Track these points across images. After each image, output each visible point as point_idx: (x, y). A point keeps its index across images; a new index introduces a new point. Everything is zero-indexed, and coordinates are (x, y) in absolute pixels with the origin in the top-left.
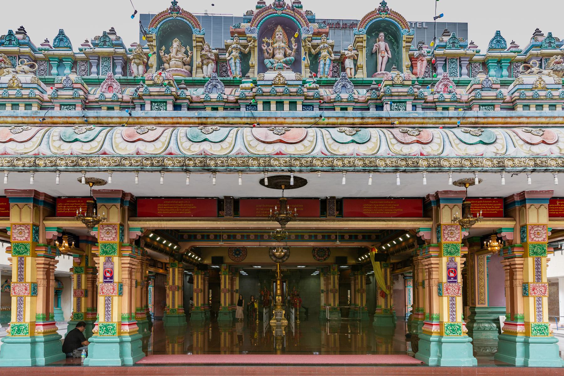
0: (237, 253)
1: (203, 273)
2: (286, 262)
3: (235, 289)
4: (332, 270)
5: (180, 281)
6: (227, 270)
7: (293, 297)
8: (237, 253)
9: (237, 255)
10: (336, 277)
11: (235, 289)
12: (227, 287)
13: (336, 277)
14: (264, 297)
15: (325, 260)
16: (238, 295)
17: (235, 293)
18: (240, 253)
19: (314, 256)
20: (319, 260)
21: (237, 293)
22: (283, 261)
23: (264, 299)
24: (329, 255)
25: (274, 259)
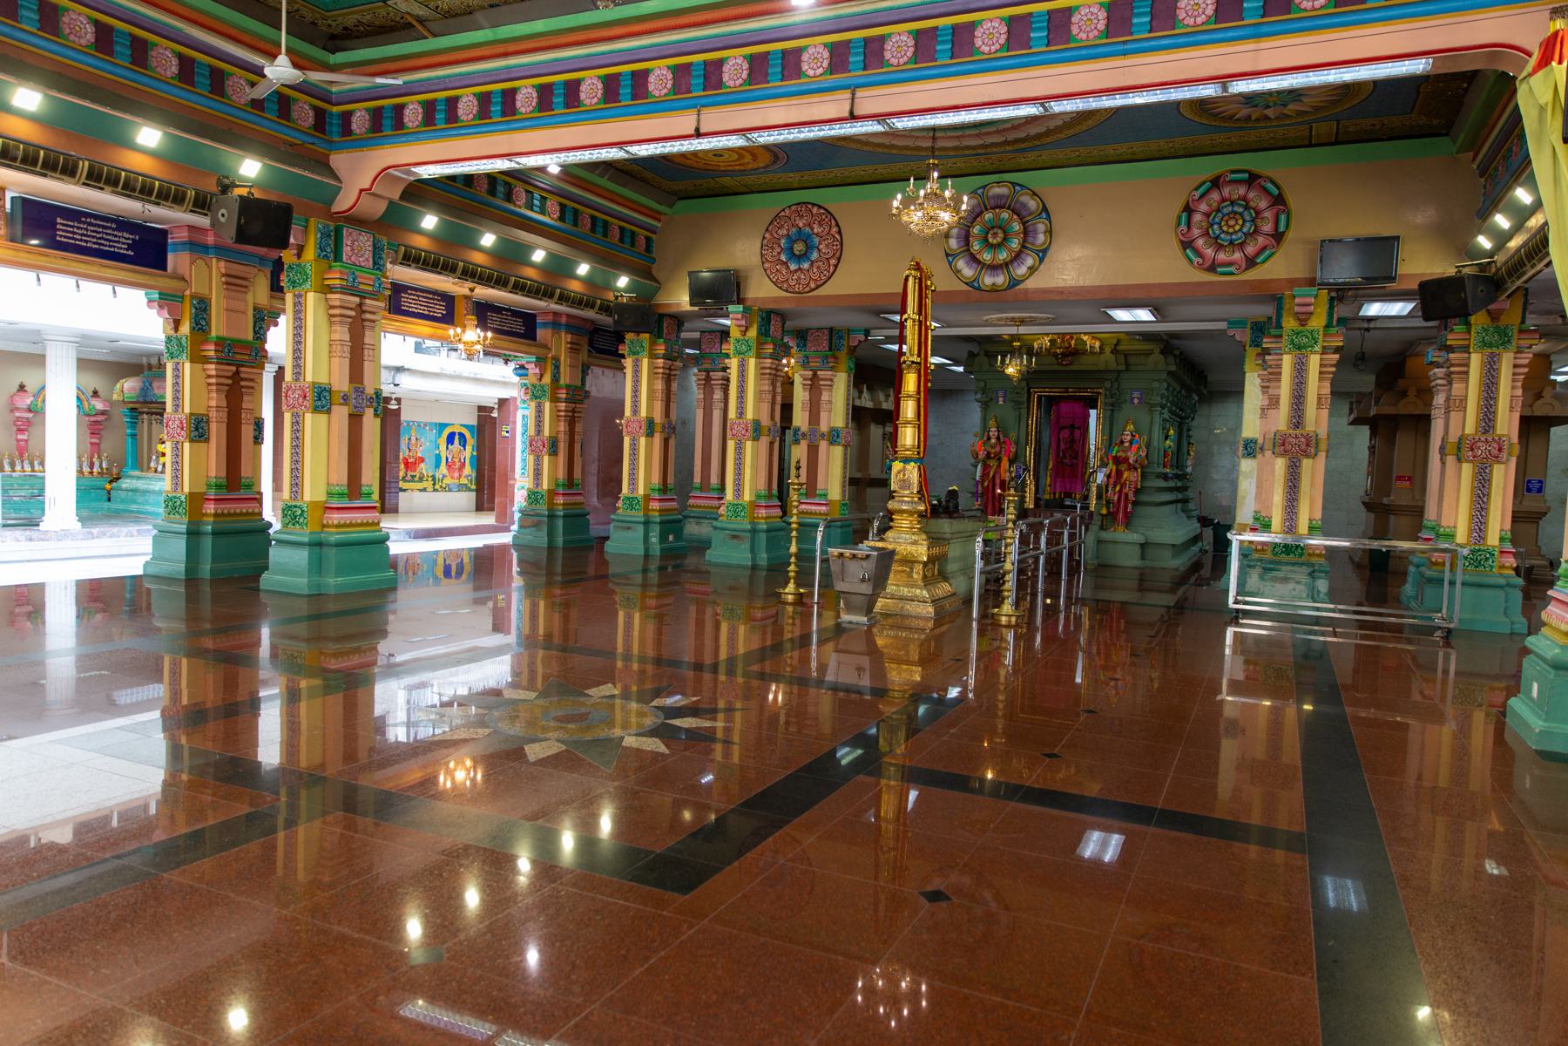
0: (799, 248)
1: (661, 350)
2: (1031, 284)
3: (824, 428)
4: (1289, 323)
5: (766, 407)
6: (753, 333)
7: (1119, 474)
8: (799, 248)
9: (799, 258)
10: (1314, 361)
11: (824, 428)
12: (750, 415)
13: (1314, 361)
14: (986, 467)
15: (1251, 262)
16: (838, 451)
17: (823, 445)
18: (809, 247)
19: (1187, 244)
20: (1212, 268)
21: (832, 443)
22: (1014, 283)
23: (985, 475)
24: (1278, 237)
25: (968, 272)
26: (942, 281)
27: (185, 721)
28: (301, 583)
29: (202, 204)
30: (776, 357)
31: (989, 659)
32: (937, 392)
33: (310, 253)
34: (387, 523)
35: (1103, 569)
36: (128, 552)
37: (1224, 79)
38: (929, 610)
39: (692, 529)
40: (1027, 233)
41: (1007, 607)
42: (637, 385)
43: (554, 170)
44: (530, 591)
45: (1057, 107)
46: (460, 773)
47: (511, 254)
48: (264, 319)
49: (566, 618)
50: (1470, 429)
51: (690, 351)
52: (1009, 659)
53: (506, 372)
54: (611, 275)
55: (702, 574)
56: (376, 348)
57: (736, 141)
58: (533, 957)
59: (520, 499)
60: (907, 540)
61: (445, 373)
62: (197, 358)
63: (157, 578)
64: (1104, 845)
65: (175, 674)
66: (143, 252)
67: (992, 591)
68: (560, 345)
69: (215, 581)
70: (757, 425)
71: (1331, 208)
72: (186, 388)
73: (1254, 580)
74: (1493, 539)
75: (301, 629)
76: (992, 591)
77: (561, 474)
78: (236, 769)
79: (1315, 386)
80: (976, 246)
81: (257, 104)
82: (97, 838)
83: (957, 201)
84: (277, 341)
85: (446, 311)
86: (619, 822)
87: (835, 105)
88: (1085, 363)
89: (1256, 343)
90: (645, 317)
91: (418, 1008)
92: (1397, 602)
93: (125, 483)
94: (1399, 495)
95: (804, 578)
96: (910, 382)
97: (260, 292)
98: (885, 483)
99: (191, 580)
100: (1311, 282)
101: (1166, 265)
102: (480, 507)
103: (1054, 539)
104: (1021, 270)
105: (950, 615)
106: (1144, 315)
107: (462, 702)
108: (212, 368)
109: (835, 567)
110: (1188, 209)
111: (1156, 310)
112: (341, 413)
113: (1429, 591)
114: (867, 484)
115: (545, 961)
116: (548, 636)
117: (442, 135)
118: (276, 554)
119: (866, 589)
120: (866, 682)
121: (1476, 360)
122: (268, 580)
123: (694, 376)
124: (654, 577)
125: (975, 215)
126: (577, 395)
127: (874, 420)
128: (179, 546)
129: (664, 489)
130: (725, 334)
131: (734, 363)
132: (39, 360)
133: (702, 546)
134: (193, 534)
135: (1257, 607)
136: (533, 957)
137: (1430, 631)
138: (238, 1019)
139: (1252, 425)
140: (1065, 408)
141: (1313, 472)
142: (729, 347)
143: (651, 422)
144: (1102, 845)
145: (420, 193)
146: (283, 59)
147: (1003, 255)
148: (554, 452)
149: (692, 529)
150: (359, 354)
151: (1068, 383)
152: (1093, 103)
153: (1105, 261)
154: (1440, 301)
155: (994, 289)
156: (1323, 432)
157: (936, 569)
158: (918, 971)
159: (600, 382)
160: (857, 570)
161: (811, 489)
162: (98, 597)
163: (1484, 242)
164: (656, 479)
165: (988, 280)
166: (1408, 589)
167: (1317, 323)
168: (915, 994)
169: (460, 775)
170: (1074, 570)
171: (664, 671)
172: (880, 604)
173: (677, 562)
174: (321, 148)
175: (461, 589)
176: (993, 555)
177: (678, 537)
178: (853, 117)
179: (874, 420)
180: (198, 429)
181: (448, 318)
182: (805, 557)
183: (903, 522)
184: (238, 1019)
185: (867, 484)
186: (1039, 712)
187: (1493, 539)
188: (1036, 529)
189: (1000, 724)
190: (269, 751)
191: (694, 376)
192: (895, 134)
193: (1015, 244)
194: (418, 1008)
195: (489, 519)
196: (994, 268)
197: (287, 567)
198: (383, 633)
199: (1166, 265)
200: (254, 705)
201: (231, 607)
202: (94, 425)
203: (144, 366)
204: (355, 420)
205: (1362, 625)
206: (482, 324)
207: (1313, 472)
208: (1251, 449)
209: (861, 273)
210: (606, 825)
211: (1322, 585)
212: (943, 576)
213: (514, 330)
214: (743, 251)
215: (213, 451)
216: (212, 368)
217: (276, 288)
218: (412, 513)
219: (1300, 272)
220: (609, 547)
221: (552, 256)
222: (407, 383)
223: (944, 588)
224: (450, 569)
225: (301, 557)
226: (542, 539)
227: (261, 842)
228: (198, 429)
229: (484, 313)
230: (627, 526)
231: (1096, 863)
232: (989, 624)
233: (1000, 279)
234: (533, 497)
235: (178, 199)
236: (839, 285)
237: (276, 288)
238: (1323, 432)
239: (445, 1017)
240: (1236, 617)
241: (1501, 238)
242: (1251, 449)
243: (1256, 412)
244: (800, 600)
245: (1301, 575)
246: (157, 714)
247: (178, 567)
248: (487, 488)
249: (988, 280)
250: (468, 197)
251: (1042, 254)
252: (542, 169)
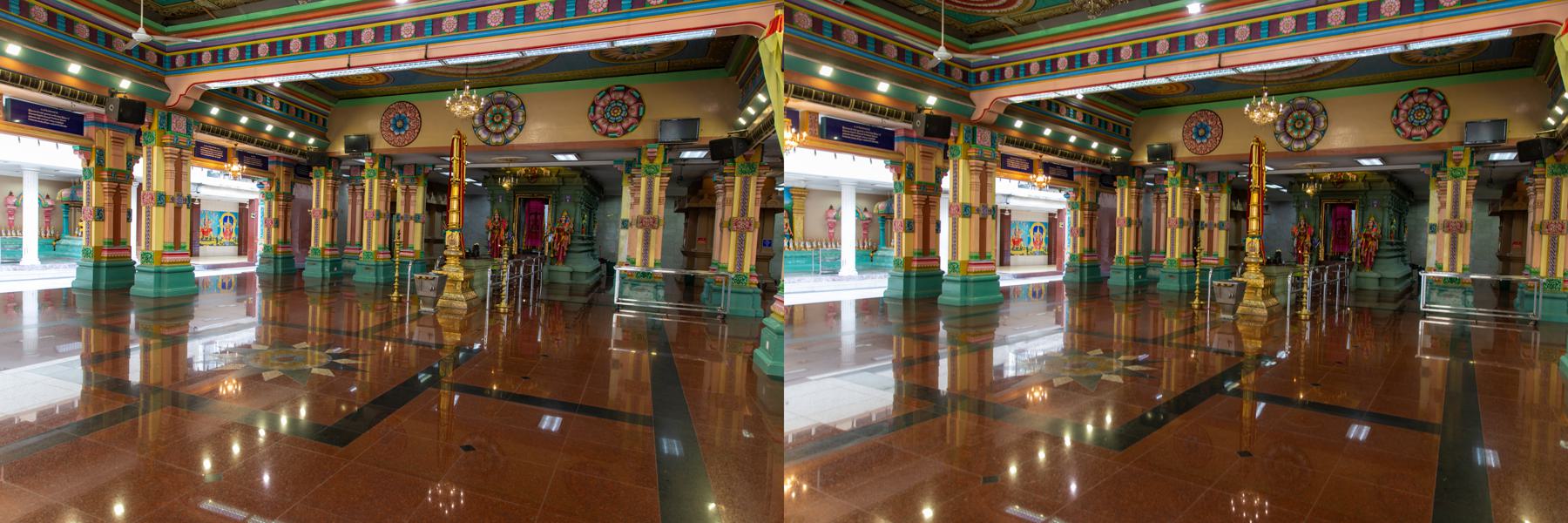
25: (484, 136)
26: (471, 140)
27: (92, 360)
28: (151, 292)
29: (101, 102)
30: (388, 178)
31: (495, 329)
32: (469, 196)
33: (155, 126)
34: (193, 262)
35: (551, 285)
36: (64, 276)
37: (612, 39)
38: (465, 305)
39: (346, 264)
40: (513, 116)
41: (504, 304)
42: (318, 192)
43: (277, 85)
44: (265, 296)
45: (529, 54)
46: (230, 387)
47: (255, 127)
48: (132, 160)
49: (283, 309)
50: (735, 214)
51: (345, 176)
52: (504, 330)
53: (251, 186)
54: (306, 137)
55: (351, 287)
56: (188, 174)
57: (368, 71)
58: (266, 479)
59: (260, 249)
60: (454, 270)
61: (222, 186)
62: (99, 179)
63: (79, 289)
64: (552, 422)
65: (88, 337)
66: (71, 126)
67: (496, 296)
68: (280, 173)
69: (108, 291)
70: (378, 213)
71: (666, 104)
72: (93, 194)
73: (627, 290)
74: (746, 270)
75: (151, 314)
76: (496, 296)
77: (281, 237)
78: (118, 385)
79: (658, 193)
80: (488, 123)
81: (129, 52)
82: (48, 419)
83: (479, 100)
84: (139, 170)
85: (223, 156)
86: (309, 411)
87: (418, 53)
88: (542, 182)
89: (628, 171)
90: (323, 159)
91: (209, 504)
92: (698, 301)
93: (63, 242)
94: (699, 248)
95: (402, 289)
96: (455, 191)
97: (130, 146)
98: (443, 241)
99: (96, 290)
100: (656, 141)
101: (583, 133)
102: (240, 254)
103: (527, 270)
104: (511, 135)
105: (475, 307)
106: (572, 157)
107: (231, 351)
108: (106, 184)
109: (417, 284)
110: (594, 105)
111: (578, 155)
112: (171, 206)
113: (715, 295)
114: (434, 242)
115: (273, 481)
116: (274, 318)
117: (221, 67)
118: (138, 277)
119: (433, 294)
120: (433, 341)
121: (738, 180)
122: (134, 290)
123: (347, 188)
124: (327, 288)
125: (487, 107)
126: (289, 198)
127: (437, 210)
128: (90, 273)
129: (332, 244)
130: (362, 167)
131: (367, 182)
132: (19, 180)
133: (351, 273)
134: (97, 267)
135: (628, 303)
136: (266, 479)
137: (715, 315)
138: (119, 509)
139: (626, 213)
140: (533, 204)
141: (657, 236)
142: (365, 174)
143: (325, 211)
144: (551, 423)
145: (210, 96)
146: (141, 30)
147: (502, 128)
148: (277, 226)
149: (346, 264)
150: (179, 177)
151: (534, 192)
152: (547, 52)
153: (553, 131)
154: (720, 150)
155: (497, 145)
156: (661, 216)
157: (468, 284)
158: (459, 485)
159: (300, 191)
160: (429, 285)
161: (405, 245)
162: (49, 298)
163: (742, 121)
164: (328, 239)
165: (494, 140)
166: (704, 295)
167: (659, 161)
168: (457, 497)
169: (230, 388)
170: (537, 285)
171: (332, 335)
172: (440, 302)
173: (338, 281)
174: (160, 74)
175: (230, 295)
176: (496, 278)
177: (339, 268)
178: (426, 59)
179: (437, 210)
180: (99, 215)
181: (224, 159)
182: (402, 279)
183: (451, 261)
184: (119, 509)
185: (434, 242)
186: (520, 356)
187: (746, 270)
188: (518, 264)
189: (500, 362)
190: (135, 375)
191: (347, 188)
192: (448, 67)
193: (507, 122)
194: (209, 504)
195: (244, 260)
196: (497, 134)
197: (144, 284)
198: (192, 317)
199: (583, 133)
200: (127, 352)
201: (116, 303)
202: (47, 213)
203: (72, 183)
204: (178, 210)
205: (681, 312)
206: (241, 162)
207: (657, 236)
208: (625, 224)
209: (430, 137)
210: (303, 412)
211: (661, 293)
212: (472, 288)
213: (257, 165)
214: (371, 125)
215: (107, 226)
216: (106, 184)
217: (138, 144)
218: (206, 256)
219: (650, 136)
220: (305, 273)
221: (276, 128)
222: (204, 192)
223: (472, 294)
224: (225, 285)
225: (151, 278)
226: (271, 270)
227: (131, 421)
228: (99, 215)
229: (242, 156)
230: (314, 263)
231: (548, 431)
232: (494, 312)
233: (500, 140)
234: (266, 248)
235: (89, 100)
236: (420, 143)
237: (138, 144)
238: (661, 216)
239: (223, 509)
240: (618, 308)
241: (751, 119)
242: (625, 224)
243: (628, 206)
244: (400, 300)
245: (651, 287)
246: (78, 357)
247: (89, 284)
248: (244, 244)
249: (494, 140)
250: (235, 99)
251: (521, 127)
252: (271, 85)
